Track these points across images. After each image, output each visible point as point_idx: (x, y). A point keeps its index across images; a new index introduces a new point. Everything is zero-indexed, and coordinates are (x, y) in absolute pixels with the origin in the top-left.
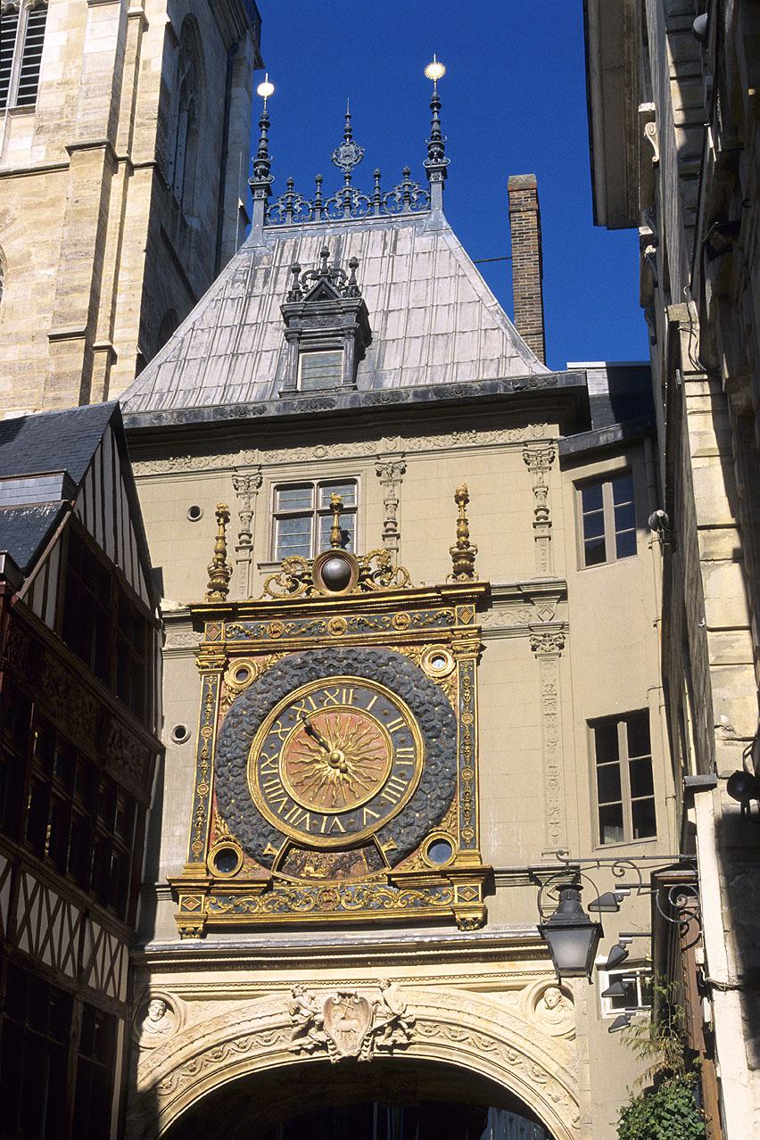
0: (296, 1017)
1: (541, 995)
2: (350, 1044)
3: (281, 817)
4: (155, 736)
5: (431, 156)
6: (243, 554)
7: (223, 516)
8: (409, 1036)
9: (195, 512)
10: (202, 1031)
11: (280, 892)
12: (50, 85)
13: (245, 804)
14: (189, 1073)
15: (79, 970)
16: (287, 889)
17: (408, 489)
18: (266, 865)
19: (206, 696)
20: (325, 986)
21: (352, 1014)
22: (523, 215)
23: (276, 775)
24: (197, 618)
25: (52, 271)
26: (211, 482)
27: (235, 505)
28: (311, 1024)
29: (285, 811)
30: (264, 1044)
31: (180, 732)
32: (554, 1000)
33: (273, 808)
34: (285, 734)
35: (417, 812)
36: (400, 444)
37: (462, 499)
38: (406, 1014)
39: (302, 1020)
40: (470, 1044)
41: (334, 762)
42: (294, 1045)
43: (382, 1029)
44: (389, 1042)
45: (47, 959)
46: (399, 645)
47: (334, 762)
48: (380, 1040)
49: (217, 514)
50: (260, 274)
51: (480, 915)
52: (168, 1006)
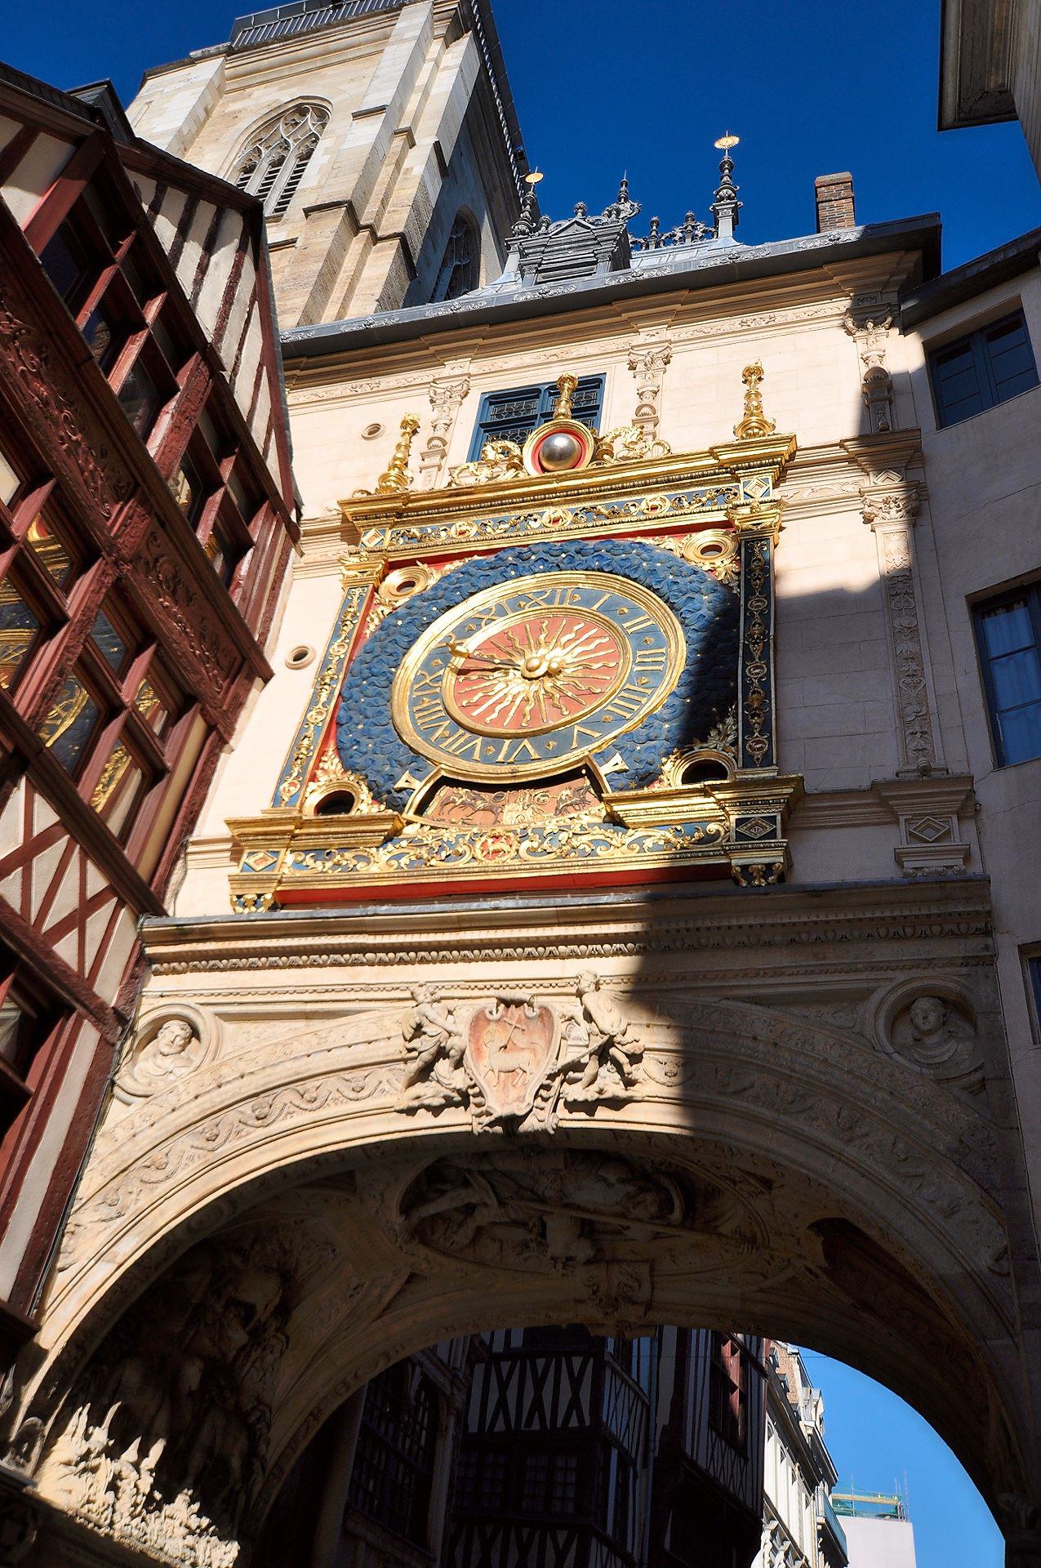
0: (415, 1043)
1: (902, 1011)
2: (513, 1094)
7: (411, 428)
8: (629, 1083)
9: (375, 430)
10: (243, 1067)
11: (411, 841)
12: (304, 190)
14: (202, 1143)
17: (671, 378)
19: (347, 603)
20: (476, 993)
21: (520, 1039)
22: (835, 204)
28: (441, 1053)
30: (353, 1095)
31: (300, 656)
32: (932, 1018)
33: (427, 734)
35: (666, 721)
36: (664, 333)
37: (753, 374)
38: (628, 1038)
39: (426, 1045)
40: (756, 1099)
42: (406, 1099)
43: (577, 1066)
44: (591, 1094)
48: (575, 1092)
49: (404, 424)
51: (776, 858)
52: (195, 1033)
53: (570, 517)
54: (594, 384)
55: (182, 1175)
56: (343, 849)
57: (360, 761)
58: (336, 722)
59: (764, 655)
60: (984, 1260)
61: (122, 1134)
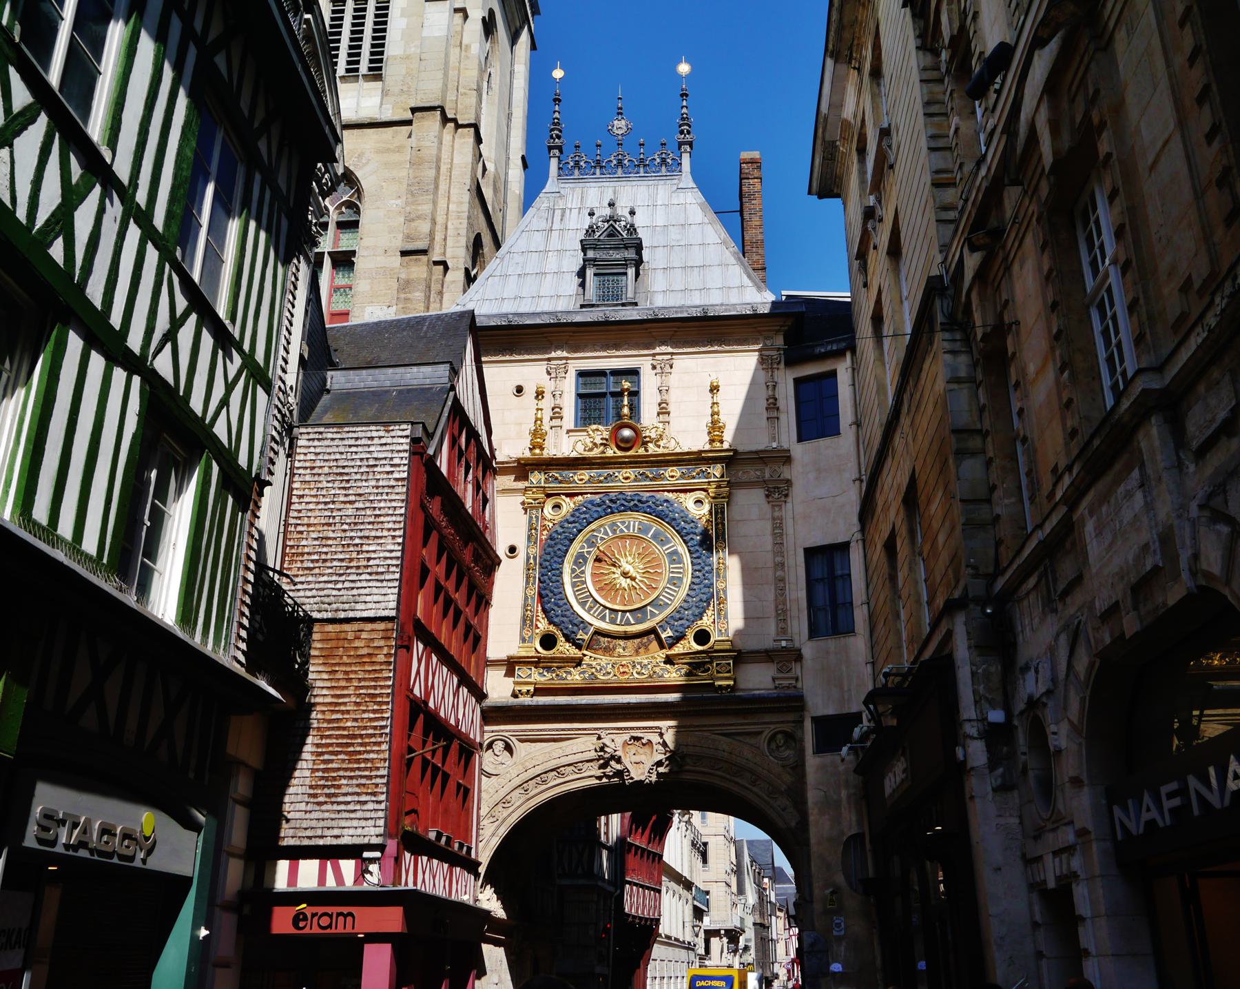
1: (772, 738)
3: (588, 611)
4: (495, 552)
5: (682, 132)
6: (556, 422)
7: (539, 394)
9: (519, 390)
13: (561, 603)
15: (457, 720)
16: (594, 663)
17: (673, 380)
18: (579, 647)
23: (584, 582)
24: (522, 469)
25: (399, 202)
26: (529, 371)
27: (549, 386)
28: (612, 757)
29: (591, 608)
31: (512, 549)
33: (583, 604)
34: (589, 553)
41: (625, 575)
42: (599, 773)
45: (442, 714)
46: (669, 491)
47: (625, 575)
48: (661, 770)
50: (558, 213)
53: (633, 477)
54: (634, 373)
55: (518, 804)
56: (558, 668)
57: (556, 620)
58: (541, 596)
59: (725, 577)
60: (793, 824)
61: (492, 791)
